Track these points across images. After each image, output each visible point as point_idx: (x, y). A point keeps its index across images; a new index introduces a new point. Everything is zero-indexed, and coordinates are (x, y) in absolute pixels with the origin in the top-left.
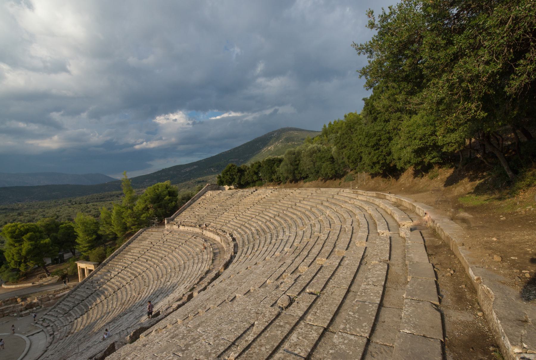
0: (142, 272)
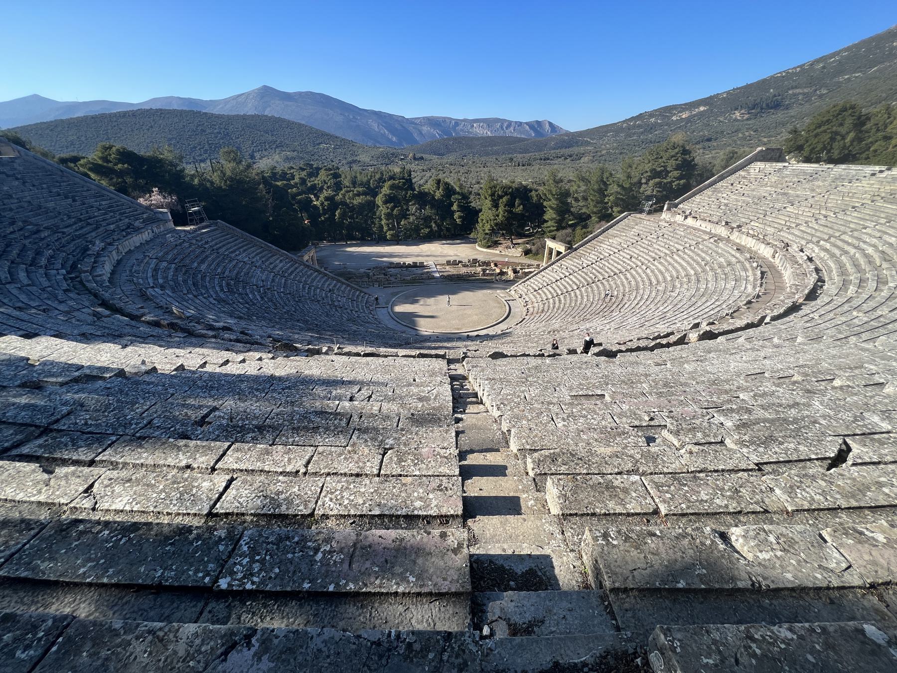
0: (624, 270)
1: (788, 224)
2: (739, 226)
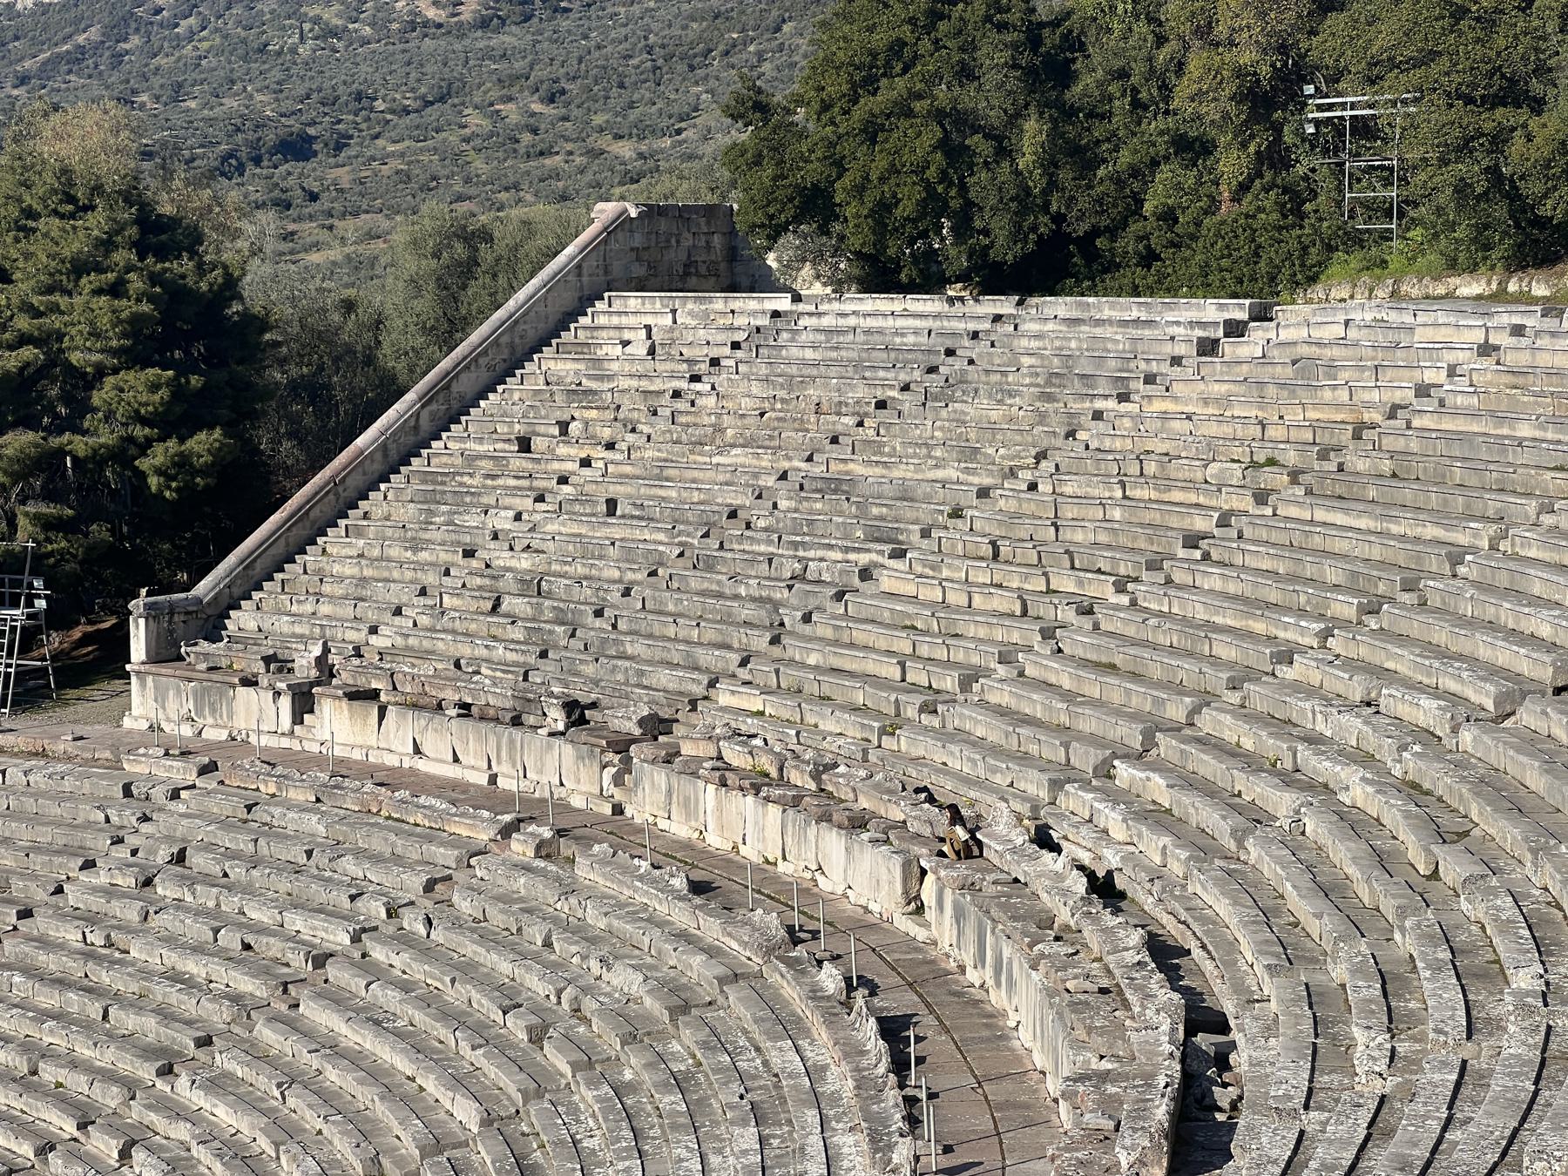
1: (917, 676)
2: (656, 726)
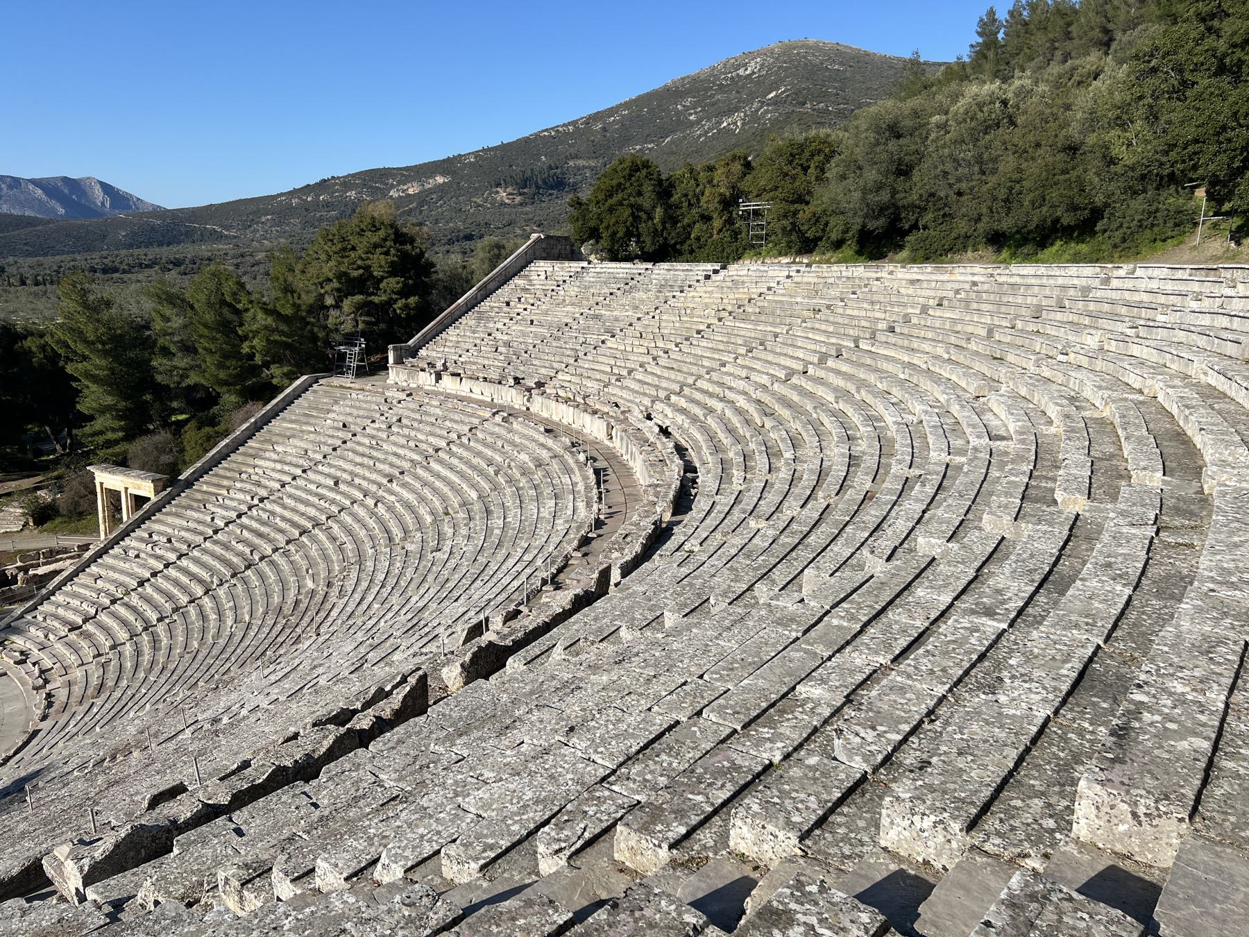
0: (324, 518)
1: (616, 371)
2: (540, 385)
